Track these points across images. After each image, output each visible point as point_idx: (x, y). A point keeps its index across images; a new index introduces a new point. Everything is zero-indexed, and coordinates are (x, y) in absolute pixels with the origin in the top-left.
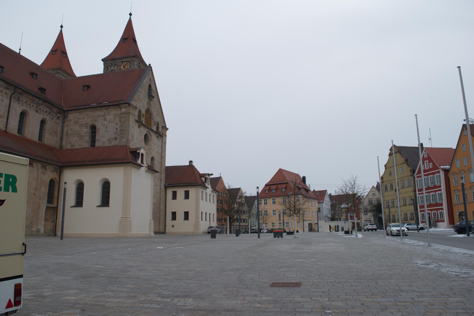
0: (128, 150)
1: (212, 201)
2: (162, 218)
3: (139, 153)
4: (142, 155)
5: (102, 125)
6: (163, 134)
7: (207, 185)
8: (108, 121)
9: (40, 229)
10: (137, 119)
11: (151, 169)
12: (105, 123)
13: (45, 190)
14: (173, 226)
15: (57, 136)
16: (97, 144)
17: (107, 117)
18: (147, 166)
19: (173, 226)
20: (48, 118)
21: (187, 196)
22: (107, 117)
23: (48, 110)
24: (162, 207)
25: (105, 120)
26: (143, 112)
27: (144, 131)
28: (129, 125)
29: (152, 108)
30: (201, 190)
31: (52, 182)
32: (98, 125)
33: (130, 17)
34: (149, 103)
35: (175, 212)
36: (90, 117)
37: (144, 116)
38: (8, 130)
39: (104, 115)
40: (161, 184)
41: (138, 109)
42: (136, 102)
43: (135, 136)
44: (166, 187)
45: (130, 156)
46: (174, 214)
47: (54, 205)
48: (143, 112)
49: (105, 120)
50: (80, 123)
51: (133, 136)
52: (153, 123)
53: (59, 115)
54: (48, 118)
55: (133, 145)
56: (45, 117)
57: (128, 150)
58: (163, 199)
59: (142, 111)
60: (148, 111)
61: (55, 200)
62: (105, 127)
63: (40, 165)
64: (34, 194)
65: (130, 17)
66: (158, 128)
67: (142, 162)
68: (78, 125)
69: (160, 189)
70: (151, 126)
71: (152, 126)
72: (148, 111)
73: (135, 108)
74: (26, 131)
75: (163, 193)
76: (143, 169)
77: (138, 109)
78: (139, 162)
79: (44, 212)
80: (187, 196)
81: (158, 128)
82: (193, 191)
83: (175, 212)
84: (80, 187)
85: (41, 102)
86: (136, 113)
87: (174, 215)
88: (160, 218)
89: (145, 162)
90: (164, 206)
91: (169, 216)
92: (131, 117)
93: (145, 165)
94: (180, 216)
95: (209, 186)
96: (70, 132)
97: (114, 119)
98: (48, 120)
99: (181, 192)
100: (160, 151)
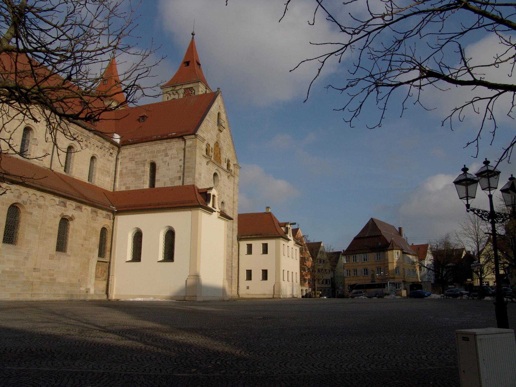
0: (197, 191)
1: (294, 257)
2: (235, 277)
3: (210, 194)
4: (214, 196)
5: (163, 162)
6: (234, 173)
7: (289, 237)
8: (170, 156)
9: (89, 289)
10: (205, 153)
11: (223, 215)
12: (167, 159)
13: (95, 240)
14: (248, 288)
15: (109, 176)
16: (157, 185)
17: (170, 152)
18: (219, 211)
19: (248, 288)
20: (98, 153)
21: (265, 250)
22: (170, 152)
23: (100, 144)
24: (235, 264)
25: (167, 155)
26: (212, 145)
27: (213, 169)
28: (195, 161)
29: (222, 141)
30: (282, 242)
31: (104, 231)
32: (159, 163)
33: (193, 38)
34: (218, 135)
35: (251, 271)
36: (148, 153)
37: (213, 150)
38: (52, 169)
39: (165, 150)
40: (233, 235)
41: (206, 142)
42: (203, 133)
43: (203, 175)
44: (240, 238)
45: (200, 199)
46: (249, 274)
47: (107, 259)
48: (212, 145)
49: (167, 155)
50: (136, 160)
51: (200, 174)
52: (223, 160)
53: (111, 151)
54: (98, 153)
55: (201, 185)
56: (96, 153)
57: (197, 191)
58: (236, 253)
59: (211, 145)
60: (217, 144)
61: (108, 253)
62: (167, 163)
63: (89, 209)
64: (83, 245)
65: (193, 38)
66: (228, 165)
67: (213, 206)
68: (134, 162)
69: (232, 241)
70: (220, 163)
71: (222, 163)
72: (217, 144)
73: (203, 140)
74: (74, 169)
75: (236, 247)
76: (216, 215)
77: (206, 142)
78: (210, 205)
79: (94, 267)
80: (265, 250)
81: (228, 165)
82: (271, 243)
83: (251, 271)
84: (138, 237)
85: (91, 135)
86: (204, 147)
87: (249, 274)
88: (232, 277)
89: (216, 206)
90: (237, 263)
91: (243, 275)
92: (197, 150)
93: (217, 210)
94: (257, 275)
95: (291, 238)
96: (124, 171)
97: (178, 155)
98: (99, 156)
99: (257, 245)
100: (232, 195)
